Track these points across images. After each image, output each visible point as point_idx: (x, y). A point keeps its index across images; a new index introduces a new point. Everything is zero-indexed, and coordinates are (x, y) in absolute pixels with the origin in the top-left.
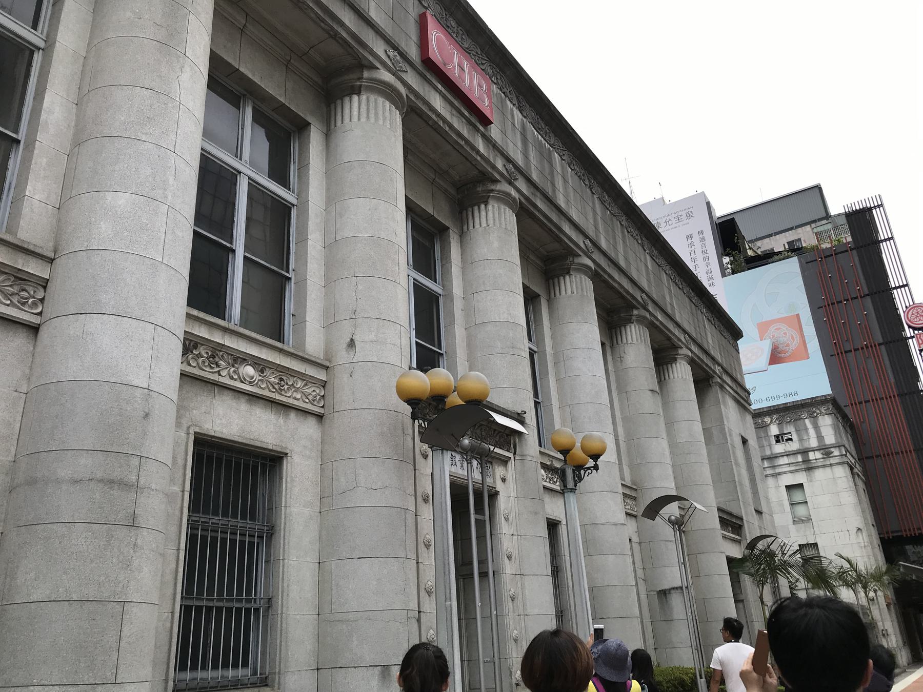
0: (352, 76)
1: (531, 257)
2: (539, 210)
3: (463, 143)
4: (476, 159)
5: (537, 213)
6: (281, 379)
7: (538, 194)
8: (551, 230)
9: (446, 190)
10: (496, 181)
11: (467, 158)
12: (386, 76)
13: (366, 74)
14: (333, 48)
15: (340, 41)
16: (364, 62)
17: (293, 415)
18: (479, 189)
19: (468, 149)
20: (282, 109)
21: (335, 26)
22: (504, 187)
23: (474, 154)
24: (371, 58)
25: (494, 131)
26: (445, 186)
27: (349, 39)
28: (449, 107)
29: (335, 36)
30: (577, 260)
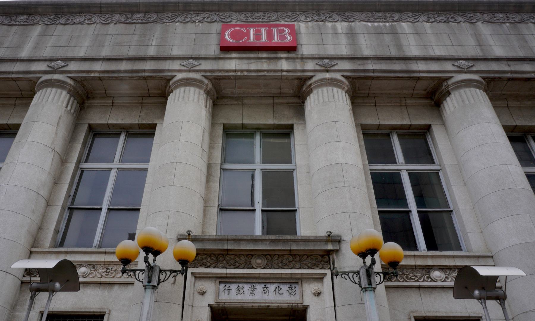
0: (168, 88)
2: (373, 71)
3: (265, 73)
4: (284, 76)
5: (371, 74)
6: (107, 269)
7: (370, 61)
9: (287, 103)
10: (311, 77)
11: (281, 78)
12: (180, 76)
13: (171, 83)
14: (152, 84)
16: (168, 78)
17: (116, 287)
18: (304, 89)
19: (272, 74)
20: (140, 126)
21: (140, 75)
22: (320, 76)
23: (279, 74)
24: (169, 74)
25: (307, 47)
26: (285, 101)
27: (154, 75)
28: (246, 61)
29: (145, 78)
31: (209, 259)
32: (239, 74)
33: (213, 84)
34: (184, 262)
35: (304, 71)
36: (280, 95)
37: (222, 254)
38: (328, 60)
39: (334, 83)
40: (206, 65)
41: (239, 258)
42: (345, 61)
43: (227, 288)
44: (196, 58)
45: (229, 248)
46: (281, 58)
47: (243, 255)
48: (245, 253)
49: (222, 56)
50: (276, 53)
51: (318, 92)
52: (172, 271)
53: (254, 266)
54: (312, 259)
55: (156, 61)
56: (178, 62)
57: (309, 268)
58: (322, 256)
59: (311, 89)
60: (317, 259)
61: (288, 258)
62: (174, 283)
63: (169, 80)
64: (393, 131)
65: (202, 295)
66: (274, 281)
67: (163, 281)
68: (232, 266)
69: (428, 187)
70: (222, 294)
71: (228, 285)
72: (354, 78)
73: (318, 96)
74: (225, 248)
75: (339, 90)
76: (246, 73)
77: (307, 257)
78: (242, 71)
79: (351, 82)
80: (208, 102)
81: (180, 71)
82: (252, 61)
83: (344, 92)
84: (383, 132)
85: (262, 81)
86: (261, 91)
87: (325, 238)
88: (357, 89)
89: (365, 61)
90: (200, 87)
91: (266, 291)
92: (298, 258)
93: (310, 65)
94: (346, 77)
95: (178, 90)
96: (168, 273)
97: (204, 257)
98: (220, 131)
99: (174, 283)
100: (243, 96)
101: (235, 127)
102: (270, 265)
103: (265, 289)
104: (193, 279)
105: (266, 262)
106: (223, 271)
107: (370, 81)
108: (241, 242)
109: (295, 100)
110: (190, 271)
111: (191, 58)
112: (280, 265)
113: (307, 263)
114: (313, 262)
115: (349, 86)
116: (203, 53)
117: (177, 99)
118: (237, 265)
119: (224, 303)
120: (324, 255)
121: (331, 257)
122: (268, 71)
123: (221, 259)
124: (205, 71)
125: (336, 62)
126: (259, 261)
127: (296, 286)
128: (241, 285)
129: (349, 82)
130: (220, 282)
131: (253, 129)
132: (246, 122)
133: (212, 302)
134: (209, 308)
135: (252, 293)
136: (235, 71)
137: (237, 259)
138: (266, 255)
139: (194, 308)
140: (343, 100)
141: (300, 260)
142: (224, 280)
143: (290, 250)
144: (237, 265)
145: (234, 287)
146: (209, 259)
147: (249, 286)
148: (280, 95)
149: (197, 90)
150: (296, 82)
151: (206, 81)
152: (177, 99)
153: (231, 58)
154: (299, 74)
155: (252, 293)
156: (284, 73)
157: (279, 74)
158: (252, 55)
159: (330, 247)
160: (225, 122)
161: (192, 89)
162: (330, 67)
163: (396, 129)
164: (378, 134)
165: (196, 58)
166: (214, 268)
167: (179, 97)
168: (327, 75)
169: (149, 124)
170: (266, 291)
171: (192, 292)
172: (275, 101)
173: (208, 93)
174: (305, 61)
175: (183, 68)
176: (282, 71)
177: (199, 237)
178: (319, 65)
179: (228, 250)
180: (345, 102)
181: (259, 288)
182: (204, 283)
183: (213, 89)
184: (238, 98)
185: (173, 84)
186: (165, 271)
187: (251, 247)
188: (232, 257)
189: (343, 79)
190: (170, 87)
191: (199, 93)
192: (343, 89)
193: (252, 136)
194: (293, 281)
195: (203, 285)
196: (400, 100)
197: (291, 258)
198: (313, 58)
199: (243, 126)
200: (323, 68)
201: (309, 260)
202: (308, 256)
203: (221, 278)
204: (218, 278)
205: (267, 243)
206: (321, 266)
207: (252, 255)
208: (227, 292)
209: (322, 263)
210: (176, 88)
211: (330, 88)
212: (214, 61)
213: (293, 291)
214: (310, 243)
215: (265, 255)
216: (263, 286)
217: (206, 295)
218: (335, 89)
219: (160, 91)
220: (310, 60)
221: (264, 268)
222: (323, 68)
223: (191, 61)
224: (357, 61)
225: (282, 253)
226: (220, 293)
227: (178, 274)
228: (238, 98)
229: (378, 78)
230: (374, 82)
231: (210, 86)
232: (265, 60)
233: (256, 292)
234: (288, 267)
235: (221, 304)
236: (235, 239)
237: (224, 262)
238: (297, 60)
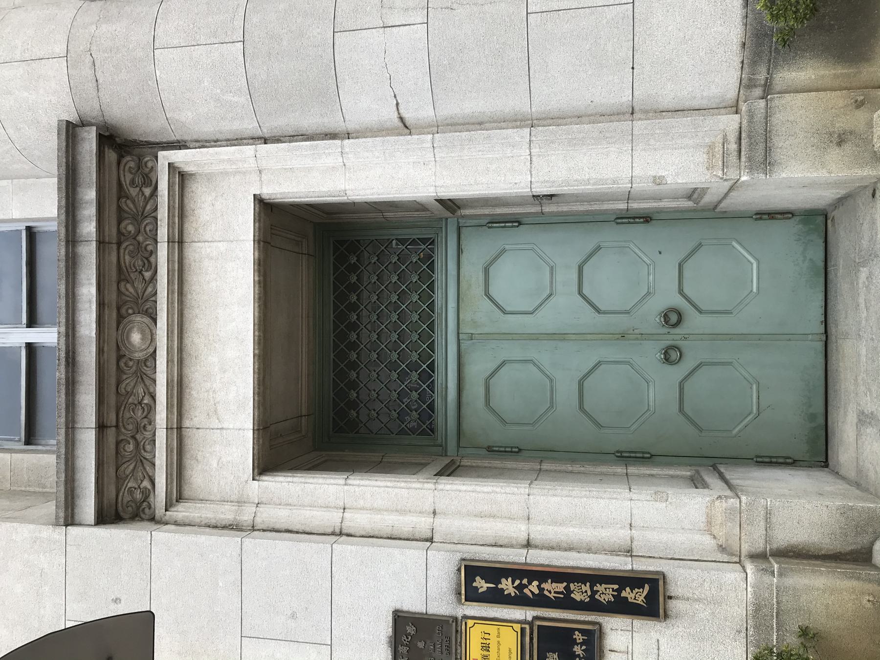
37: (118, 443)
41: (129, 394)
47: (118, 383)
53: (151, 350)
105: (138, 318)
113: (142, 199)
114: (139, 180)
126: (136, 338)
188: (127, 415)
201: (133, 192)
202: (122, 193)
207: (120, 357)
215: (120, 318)
221: (155, 321)
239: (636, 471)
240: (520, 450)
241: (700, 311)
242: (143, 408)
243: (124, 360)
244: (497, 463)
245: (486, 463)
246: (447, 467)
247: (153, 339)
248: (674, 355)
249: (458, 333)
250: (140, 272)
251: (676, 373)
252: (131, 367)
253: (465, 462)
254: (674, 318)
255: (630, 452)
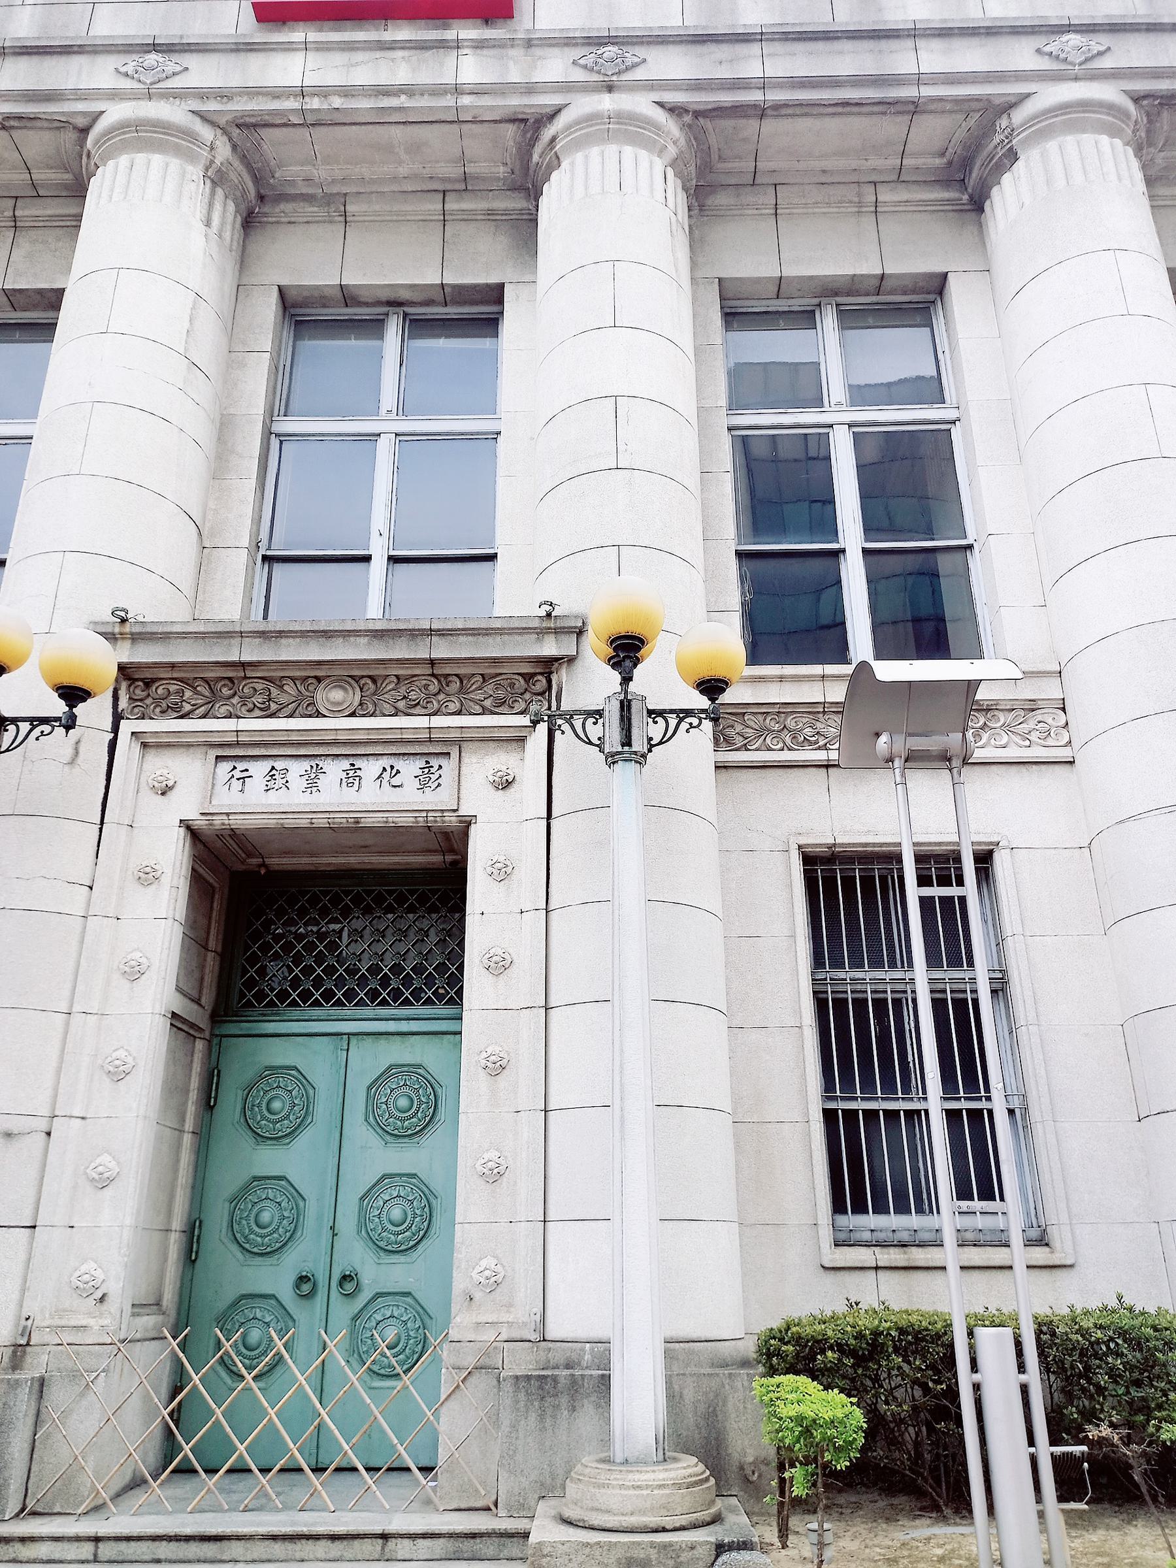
1: (886, 196)
2: (764, 84)
3: (403, 101)
5: (756, 96)
8: (846, 104)
9: (490, 212)
10: (558, 111)
12: (115, 113)
15: (12, 123)
16: (81, 122)
18: (535, 158)
23: (449, 101)
24: (80, 107)
26: (483, 205)
28: (339, 58)
30: (1019, 116)
31: (188, 694)
32: (315, 103)
33: (234, 147)
34: (73, 695)
35: (530, 89)
36: (466, 184)
37: (230, 679)
38: (614, 49)
39: (625, 128)
40: (203, 73)
42: (671, 48)
43: (237, 774)
44: (168, 49)
45: (246, 658)
46: (458, 45)
47: (293, 679)
48: (298, 674)
49: (259, 38)
50: (446, 27)
51: (572, 164)
52: (37, 721)
54: (498, 686)
55: (35, 59)
56: (110, 63)
57: (485, 711)
58: (528, 677)
59: (558, 158)
60: (512, 685)
61: (426, 686)
62: (72, 762)
63: (85, 131)
64: (824, 301)
65: (163, 794)
66: (379, 749)
67: (7, 750)
68: (257, 713)
69: (913, 476)
70: (221, 789)
71: (241, 766)
72: (697, 114)
73: (572, 179)
74: (234, 658)
75: (643, 154)
76: (337, 102)
77: (484, 680)
78: (323, 92)
79: (690, 126)
80: (218, 207)
81: (114, 95)
82: (360, 56)
83: (659, 164)
84: (796, 305)
85: (397, 132)
86: (403, 171)
87: (536, 623)
88: (715, 157)
89: (742, 49)
90: (191, 157)
91: (353, 778)
92: (455, 685)
93: (555, 67)
94: (674, 110)
95: (111, 163)
96: (25, 727)
97: (173, 688)
98: (267, 309)
99: (72, 762)
100: (345, 190)
101: (318, 297)
102: (371, 708)
103: (351, 773)
104: (137, 747)
106: (230, 724)
107: (754, 123)
108: (284, 641)
109: (517, 203)
110: (126, 727)
111: (155, 47)
112: (401, 705)
114: (501, 693)
115: (682, 142)
116: (196, 31)
117: (105, 194)
118: (274, 707)
119: (228, 814)
120: (535, 674)
121: (554, 678)
122: (408, 90)
123: (224, 690)
124: (203, 94)
125: (641, 52)
126: (337, 695)
127: (443, 761)
128: (279, 764)
129: (684, 127)
130: (219, 758)
131: (379, 303)
132: (353, 278)
133: (192, 814)
134: (182, 831)
135: (312, 786)
136: (302, 93)
137: (275, 692)
138: (363, 677)
139: (136, 831)
140: (652, 191)
141: (462, 690)
142: (230, 751)
143: (432, 662)
144: (274, 707)
145: (259, 769)
146: (188, 694)
147: (305, 765)
148: (466, 184)
149: (175, 163)
150: (510, 130)
151: (207, 133)
152: (105, 194)
153: (288, 47)
154: (515, 102)
155: (312, 786)
156: (466, 100)
157: (449, 101)
158: (360, 35)
159: (549, 648)
160: (285, 281)
161: (157, 159)
162: (619, 73)
163: (836, 293)
164: (777, 312)
165: (168, 49)
166: (204, 716)
167: (112, 190)
168: (606, 103)
169: (40, 292)
170: (353, 778)
171: (132, 787)
172: (447, 207)
173: (217, 179)
174: (538, 52)
175: (127, 84)
176: (458, 90)
177: (155, 629)
178: (585, 67)
179: (243, 665)
180: (660, 195)
181: (334, 770)
182: (170, 763)
183: (237, 163)
184: (328, 199)
185: (97, 142)
186: (14, 721)
187: (314, 652)
189: (660, 116)
190: (89, 155)
191: (183, 174)
192: (662, 151)
193: (374, 327)
194: (434, 750)
195: (163, 765)
196: (862, 191)
197: (434, 686)
198: (568, 42)
199: (348, 296)
200: (596, 77)
201: (489, 689)
203: (222, 745)
204: (212, 745)
205: (363, 641)
206: (523, 706)
207: (319, 679)
208: (236, 785)
209: (527, 696)
210: (105, 159)
211: (612, 149)
212: (233, 57)
213: (434, 777)
214: (490, 640)
216: (345, 764)
217: (172, 795)
218: (628, 150)
219: (68, 177)
220: (556, 51)
221: (353, 715)
222: (596, 77)
223: (152, 58)
224: (712, 47)
225: (409, 672)
226: (218, 787)
227: (53, 727)
228: (328, 199)
229: (779, 108)
230: (769, 126)
231: (224, 151)
232: (406, 53)
233: (323, 782)
234: (423, 711)
235: (218, 821)
236: (263, 632)
237: (235, 700)
238: (512, 52)
239: (172, 1241)
240: (212, 1108)
241: (355, 1318)
242: (264, 703)
243: (314, 681)
244: (195, 1083)
245: (197, 1067)
246: (192, 1025)
247: (336, 714)
248: (306, 1288)
249: (348, 1034)
250: (405, 697)
251: (285, 1290)
252: (307, 690)
253: (200, 1045)
254: (349, 1287)
255: (199, 1236)
